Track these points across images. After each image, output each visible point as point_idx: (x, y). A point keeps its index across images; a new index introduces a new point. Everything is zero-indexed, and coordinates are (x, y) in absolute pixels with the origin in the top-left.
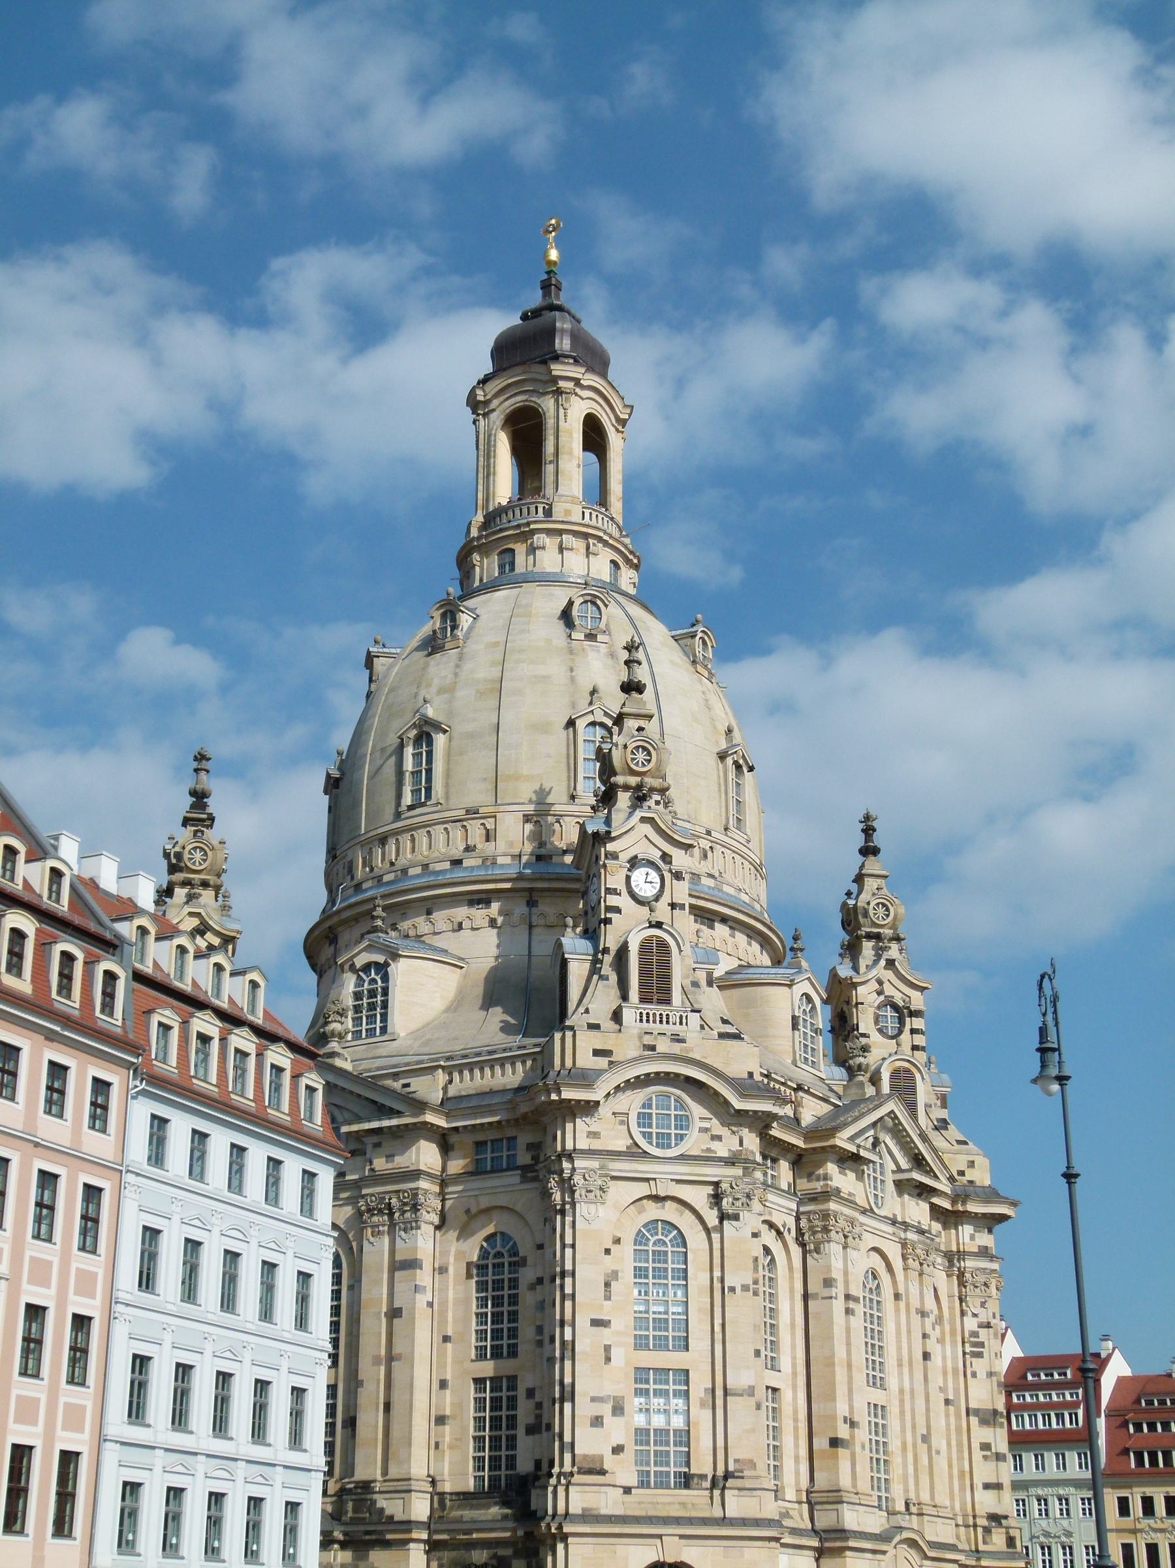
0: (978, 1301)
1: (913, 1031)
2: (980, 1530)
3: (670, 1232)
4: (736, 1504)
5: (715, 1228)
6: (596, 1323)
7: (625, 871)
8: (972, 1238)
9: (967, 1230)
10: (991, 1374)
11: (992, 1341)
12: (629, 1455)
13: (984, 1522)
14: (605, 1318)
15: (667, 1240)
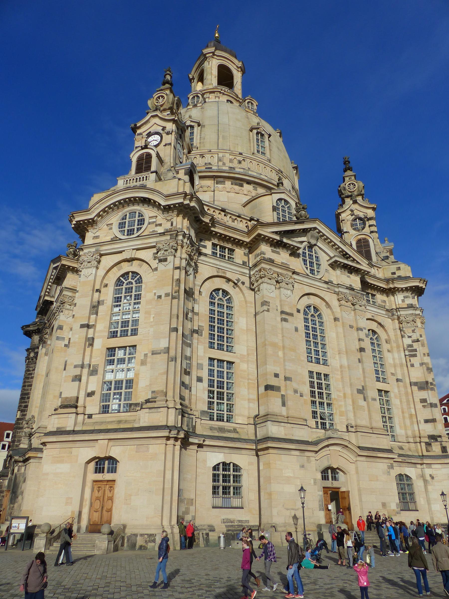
0: (410, 330)
1: (370, 226)
2: (423, 445)
3: (136, 277)
4: (145, 418)
5: (156, 269)
6: (82, 326)
7: (145, 139)
8: (403, 301)
9: (399, 297)
10: (422, 364)
11: (421, 348)
12: (97, 397)
13: (427, 440)
14: (90, 324)
15: (133, 281)
